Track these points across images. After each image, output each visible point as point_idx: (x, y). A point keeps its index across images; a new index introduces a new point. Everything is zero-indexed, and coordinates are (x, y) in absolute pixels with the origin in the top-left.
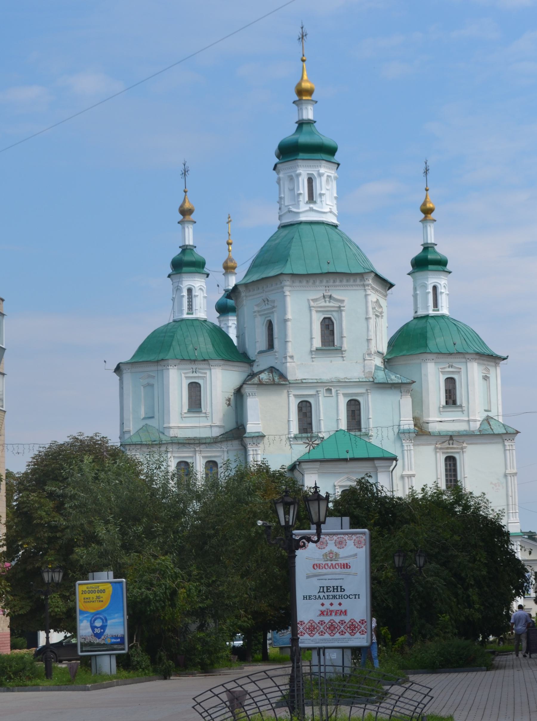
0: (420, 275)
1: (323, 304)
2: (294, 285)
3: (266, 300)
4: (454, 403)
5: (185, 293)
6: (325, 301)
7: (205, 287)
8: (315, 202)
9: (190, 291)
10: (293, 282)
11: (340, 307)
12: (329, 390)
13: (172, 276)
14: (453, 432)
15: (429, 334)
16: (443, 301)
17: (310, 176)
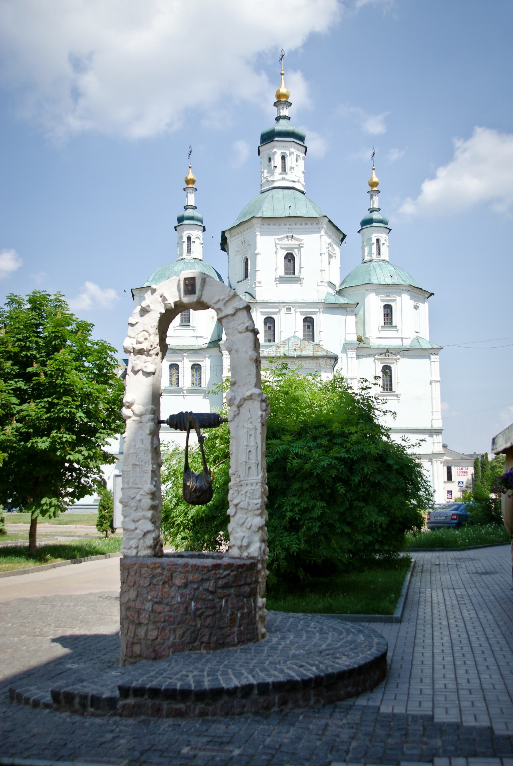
0: (367, 230)
1: (287, 242)
2: (263, 227)
3: (243, 241)
4: (391, 323)
5: (185, 239)
6: (288, 240)
7: (202, 236)
8: (287, 174)
9: (189, 238)
10: (263, 224)
11: (299, 245)
12: (289, 309)
13: (177, 228)
14: (390, 346)
15: (372, 272)
16: (384, 250)
17: (283, 154)
